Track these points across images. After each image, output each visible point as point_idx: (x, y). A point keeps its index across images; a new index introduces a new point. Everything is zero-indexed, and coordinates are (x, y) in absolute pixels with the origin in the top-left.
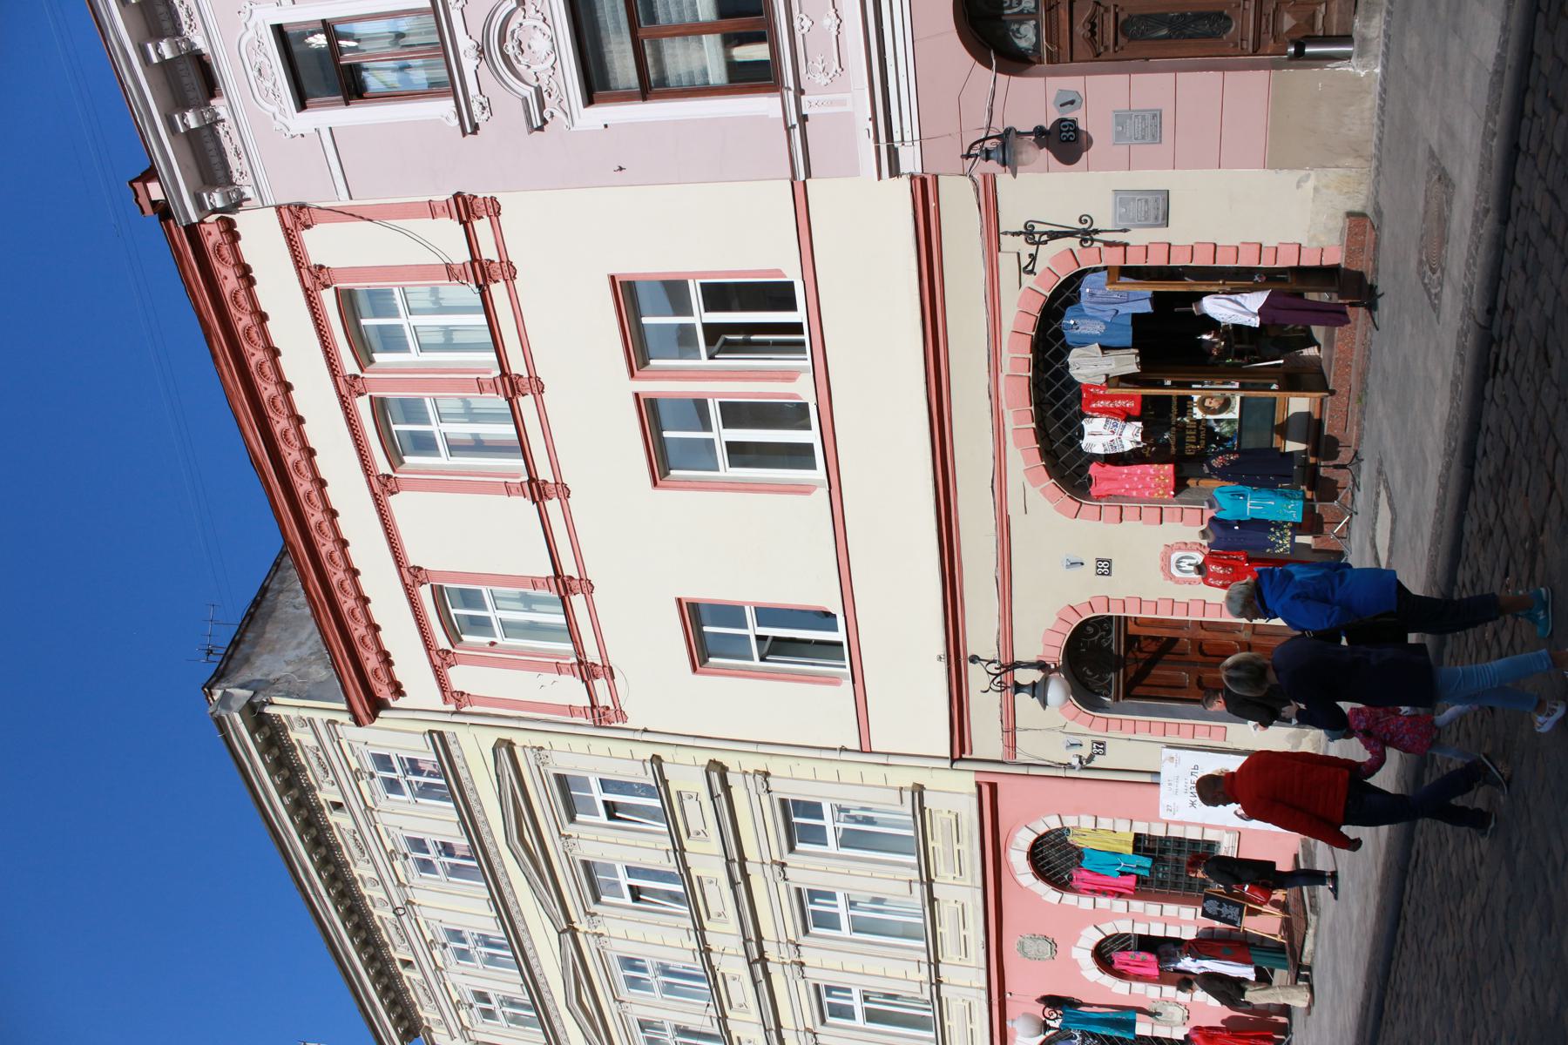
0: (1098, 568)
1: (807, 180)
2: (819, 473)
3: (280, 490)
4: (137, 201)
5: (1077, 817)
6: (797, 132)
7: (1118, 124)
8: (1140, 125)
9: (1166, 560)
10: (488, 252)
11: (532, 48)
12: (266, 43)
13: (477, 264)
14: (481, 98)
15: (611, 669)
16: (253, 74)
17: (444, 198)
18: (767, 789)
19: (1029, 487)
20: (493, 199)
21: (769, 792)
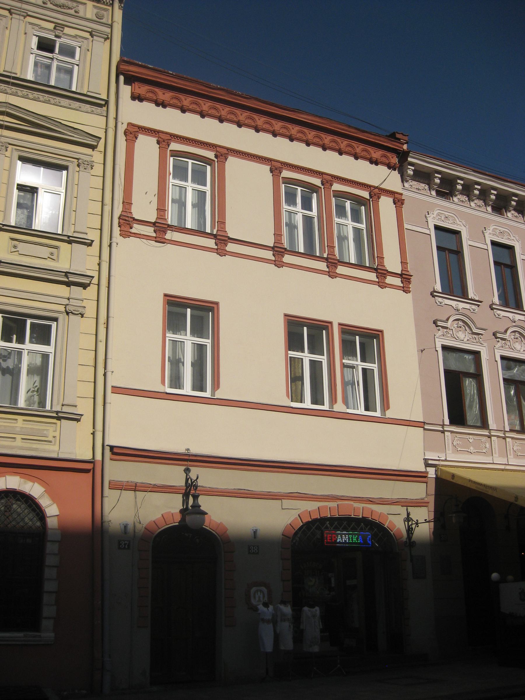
0: (254, 546)
4: (401, 134)
11: (459, 331)
12: (455, 226)
13: (385, 272)
14: (443, 304)
15: (163, 243)
18: (72, 313)
19: (299, 512)
20: (410, 292)
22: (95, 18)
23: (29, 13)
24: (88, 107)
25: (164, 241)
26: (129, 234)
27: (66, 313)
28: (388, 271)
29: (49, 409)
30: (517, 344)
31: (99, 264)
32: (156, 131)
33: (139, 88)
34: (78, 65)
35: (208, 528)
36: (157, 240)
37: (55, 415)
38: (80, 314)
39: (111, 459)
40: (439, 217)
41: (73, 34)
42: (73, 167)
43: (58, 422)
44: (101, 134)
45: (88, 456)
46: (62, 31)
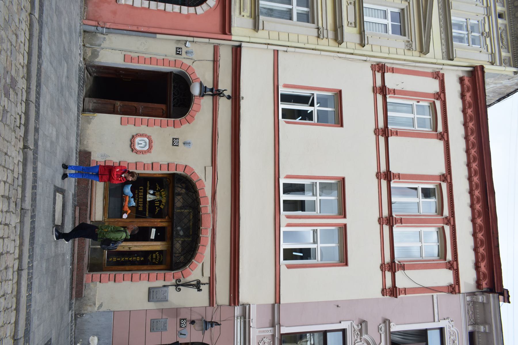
0: (178, 142)
2: (282, 181)
5: (189, 13)
7: (166, 326)
8: (158, 326)
9: (150, 147)
10: (388, 275)
14: (381, 332)
16: (456, 342)
17: (401, 296)
18: (319, 30)
19: (203, 179)
20: (383, 295)
21: (318, 28)
22: (503, 58)
23: (490, 17)
28: (396, 273)
35: (190, 109)
36: (375, 87)
40: (452, 333)
41: (487, 43)
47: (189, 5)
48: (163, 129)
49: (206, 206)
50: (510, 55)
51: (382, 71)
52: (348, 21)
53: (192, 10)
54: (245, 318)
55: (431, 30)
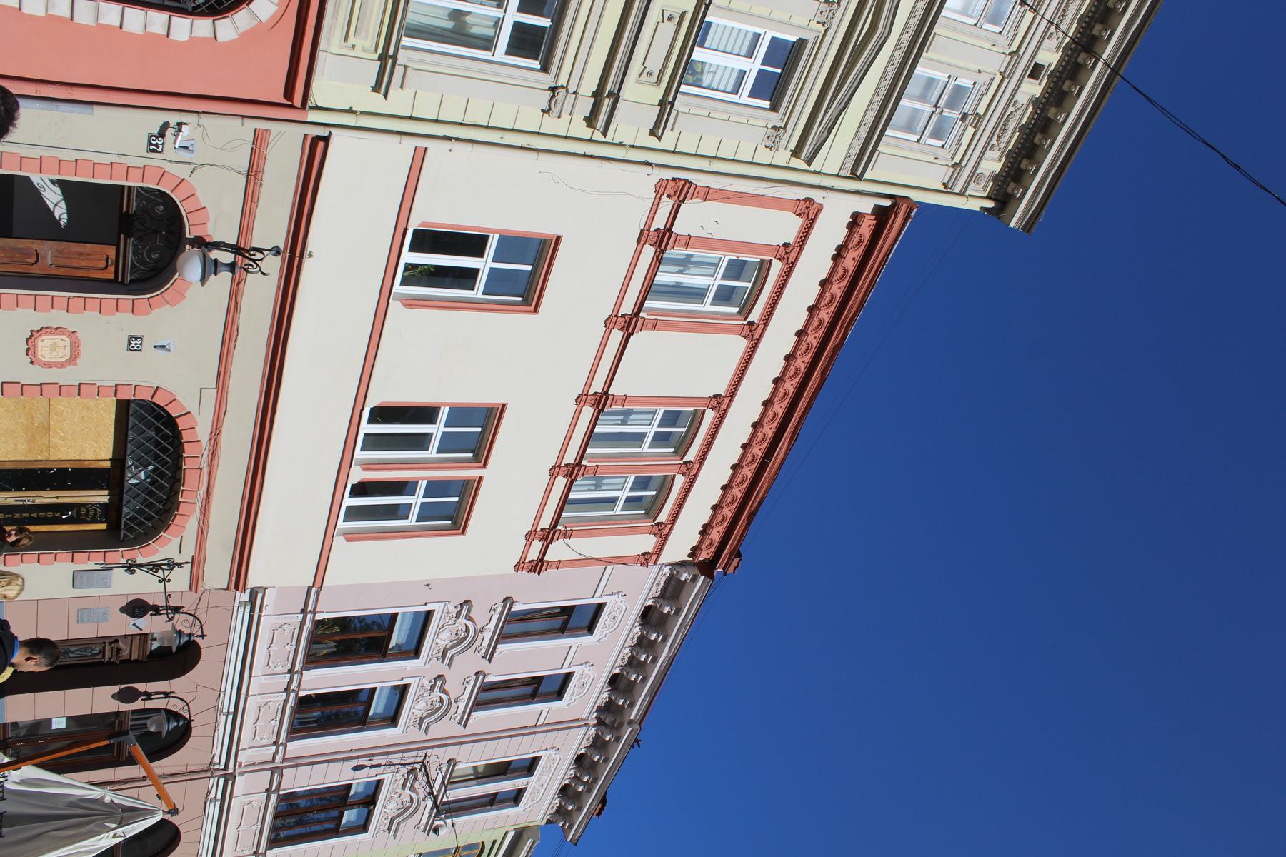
0: (141, 344)
1: (311, 585)
3: (798, 409)
4: (738, 566)
6: (310, 608)
12: (601, 629)
15: (639, 241)
18: (553, 96)
19: (194, 411)
22: (978, 171)
23: (1006, 81)
24: (856, 150)
25: (642, 242)
26: (660, 192)
27: (553, 86)
29: (403, 43)
30: (424, 705)
31: (621, 144)
32: (803, 244)
33: (869, 226)
34: (918, 141)
37: (391, 53)
38: (550, 109)
39: (306, 135)
42: (776, 119)
43: (376, 57)
44: (815, 166)
45: (318, 96)
46: (971, 125)
47: (196, 12)
48: (105, 318)
49: (194, 456)
50: (997, 167)
51: (678, 197)
52: (643, 64)
53: (203, 26)
54: (252, 610)
55: (843, 113)
